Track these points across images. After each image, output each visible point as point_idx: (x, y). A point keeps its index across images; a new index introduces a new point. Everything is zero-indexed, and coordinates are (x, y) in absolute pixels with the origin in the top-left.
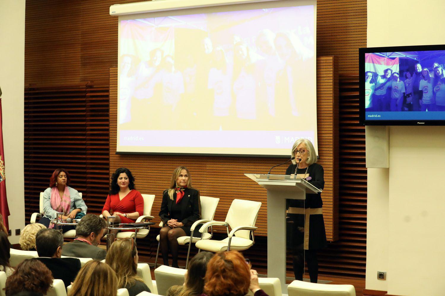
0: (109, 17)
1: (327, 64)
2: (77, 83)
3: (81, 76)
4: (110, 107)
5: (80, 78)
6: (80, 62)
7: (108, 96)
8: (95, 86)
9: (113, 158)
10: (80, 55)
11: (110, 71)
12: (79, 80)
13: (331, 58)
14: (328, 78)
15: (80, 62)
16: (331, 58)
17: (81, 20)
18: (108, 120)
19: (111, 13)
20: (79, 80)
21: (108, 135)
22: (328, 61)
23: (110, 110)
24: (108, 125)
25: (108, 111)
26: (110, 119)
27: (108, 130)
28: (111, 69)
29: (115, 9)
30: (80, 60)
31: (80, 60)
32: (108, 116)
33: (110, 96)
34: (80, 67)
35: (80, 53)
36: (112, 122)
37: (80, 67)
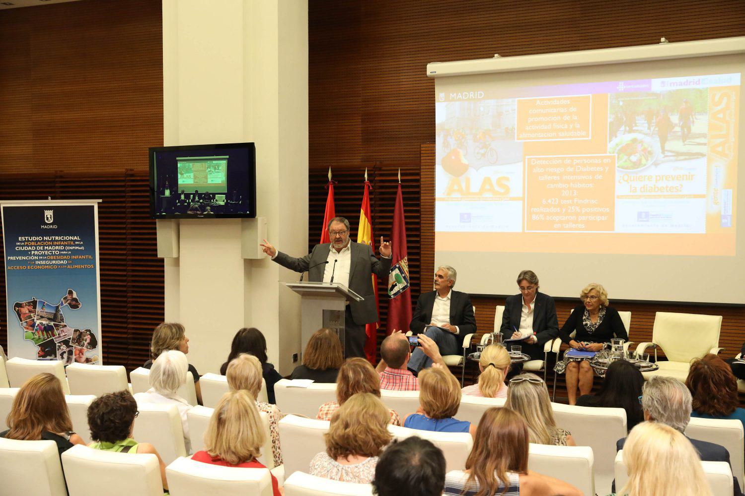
2: (356, 163)
6: (361, 138)
7: (418, 181)
17: (361, 83)
18: (418, 211)
19: (428, 73)
21: (418, 230)
23: (422, 198)
24: (419, 217)
25: (419, 199)
26: (422, 210)
27: (419, 223)
29: (434, 68)
32: (418, 205)
35: (360, 126)
36: (425, 213)
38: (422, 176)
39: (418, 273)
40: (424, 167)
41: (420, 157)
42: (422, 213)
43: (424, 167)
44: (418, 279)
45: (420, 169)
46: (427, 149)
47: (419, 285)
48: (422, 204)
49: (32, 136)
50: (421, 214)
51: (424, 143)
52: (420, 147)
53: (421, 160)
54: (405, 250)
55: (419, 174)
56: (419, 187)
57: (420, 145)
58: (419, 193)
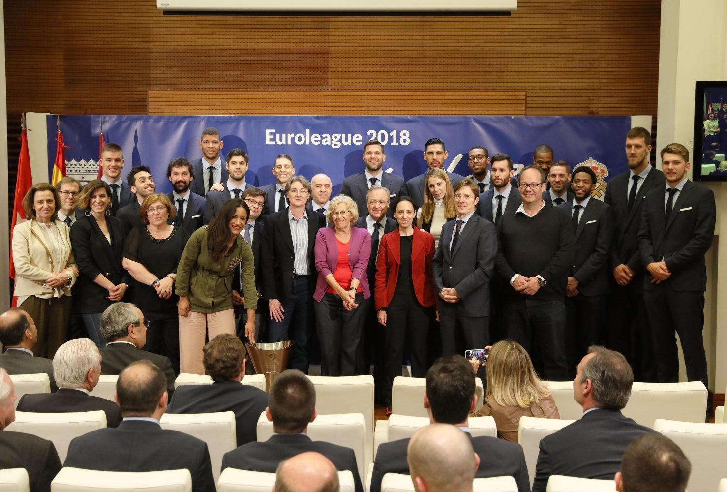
0: (155, 11)
3: (65, 99)
5: (63, 103)
10: (63, 67)
11: (150, 96)
12: (63, 106)
13: (524, 94)
16: (524, 94)
20: (63, 106)
22: (518, 98)
28: (150, 92)
30: (63, 74)
31: (63, 74)
34: (63, 85)
37: (63, 85)
46: (156, 96)
49: (152, 65)
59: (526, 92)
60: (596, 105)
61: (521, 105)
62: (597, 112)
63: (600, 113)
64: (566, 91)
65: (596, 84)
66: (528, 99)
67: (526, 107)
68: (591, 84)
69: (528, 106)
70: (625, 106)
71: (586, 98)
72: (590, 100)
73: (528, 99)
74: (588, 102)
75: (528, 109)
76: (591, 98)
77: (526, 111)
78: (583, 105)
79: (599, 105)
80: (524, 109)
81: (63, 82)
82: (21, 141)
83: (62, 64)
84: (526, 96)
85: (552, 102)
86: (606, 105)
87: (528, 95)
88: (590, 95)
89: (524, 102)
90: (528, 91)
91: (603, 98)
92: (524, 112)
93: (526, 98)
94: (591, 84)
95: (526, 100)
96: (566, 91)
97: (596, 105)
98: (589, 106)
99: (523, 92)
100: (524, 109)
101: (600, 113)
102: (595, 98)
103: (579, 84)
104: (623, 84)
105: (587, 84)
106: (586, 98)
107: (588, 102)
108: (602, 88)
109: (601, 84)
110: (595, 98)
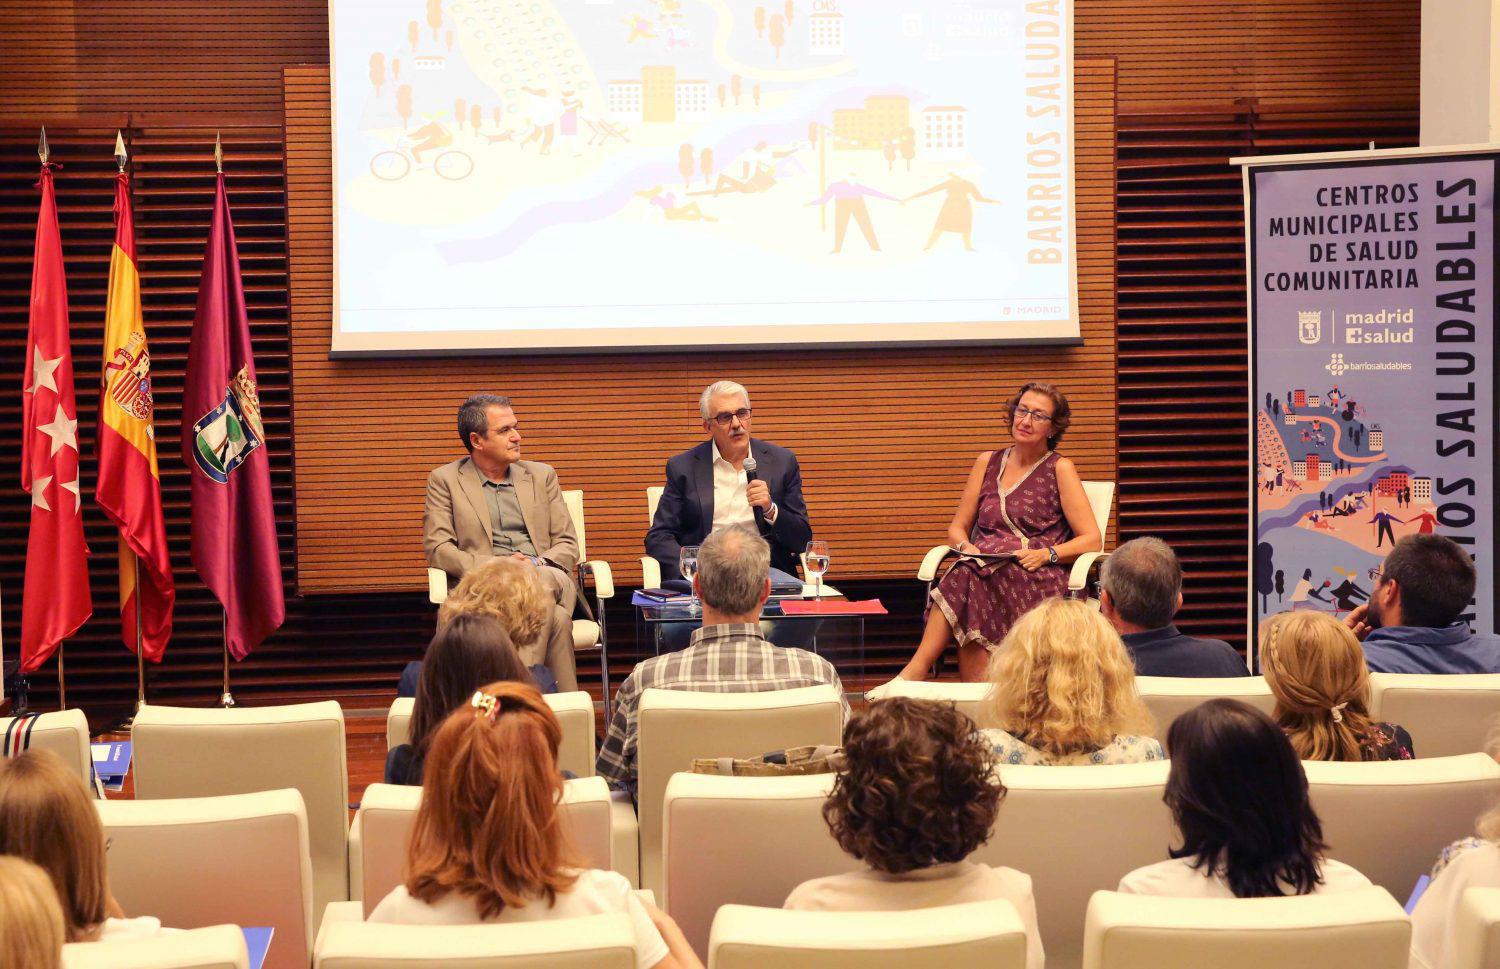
1: (1095, 79)
4: (290, 204)
7: (279, 166)
8: (148, 132)
9: (306, 371)
10: (72, 20)
13: (1111, 62)
14: (1100, 119)
15: (73, 44)
16: (1111, 62)
18: (282, 249)
21: (284, 298)
22: (1099, 71)
23: (291, 212)
24: (283, 265)
25: (282, 216)
28: (287, 72)
32: (282, 232)
33: (290, 163)
34: (73, 61)
37: (73, 61)
38: (289, 154)
39: (286, 413)
40: (296, 130)
41: (283, 101)
42: (292, 252)
43: (296, 130)
44: (288, 429)
45: (283, 135)
47: (288, 445)
48: (291, 228)
50: (288, 256)
51: (295, 64)
52: (283, 76)
53: (283, 110)
54: (248, 354)
55: (280, 149)
56: (280, 182)
57: (282, 71)
58: (282, 199)
59: (1116, 59)
60: (1250, 86)
61: (1105, 87)
62: (1255, 100)
63: (1261, 102)
64: (1188, 56)
65: (1251, 40)
66: (1120, 73)
67: (1115, 91)
68: (1237, 40)
69: (1120, 88)
70: (1309, 85)
71: (1230, 71)
72: (1238, 75)
73: (1120, 73)
74: (1238, 79)
75: (1120, 96)
76: (1239, 70)
77: (1115, 99)
78: (1222, 87)
79: (1258, 85)
80: (1112, 95)
81: (73, 52)
82: (41, 190)
83: (71, 12)
84: (1116, 68)
85: (1157, 80)
86: (1269, 86)
87: (1120, 66)
88: (1236, 64)
89: (1111, 79)
90: (1121, 58)
91: (1263, 71)
92: (1111, 103)
93: (1116, 72)
94: (1237, 40)
95: (1115, 75)
96: (1188, 56)
97: (1250, 86)
98: (1235, 87)
99: (1107, 56)
100: (1112, 95)
101: (1261, 102)
102: (1248, 70)
103: (1212, 41)
104: (1306, 39)
105: (1231, 40)
106: (1230, 71)
107: (1238, 79)
108: (1261, 48)
109: (1260, 40)
110: (1248, 70)
